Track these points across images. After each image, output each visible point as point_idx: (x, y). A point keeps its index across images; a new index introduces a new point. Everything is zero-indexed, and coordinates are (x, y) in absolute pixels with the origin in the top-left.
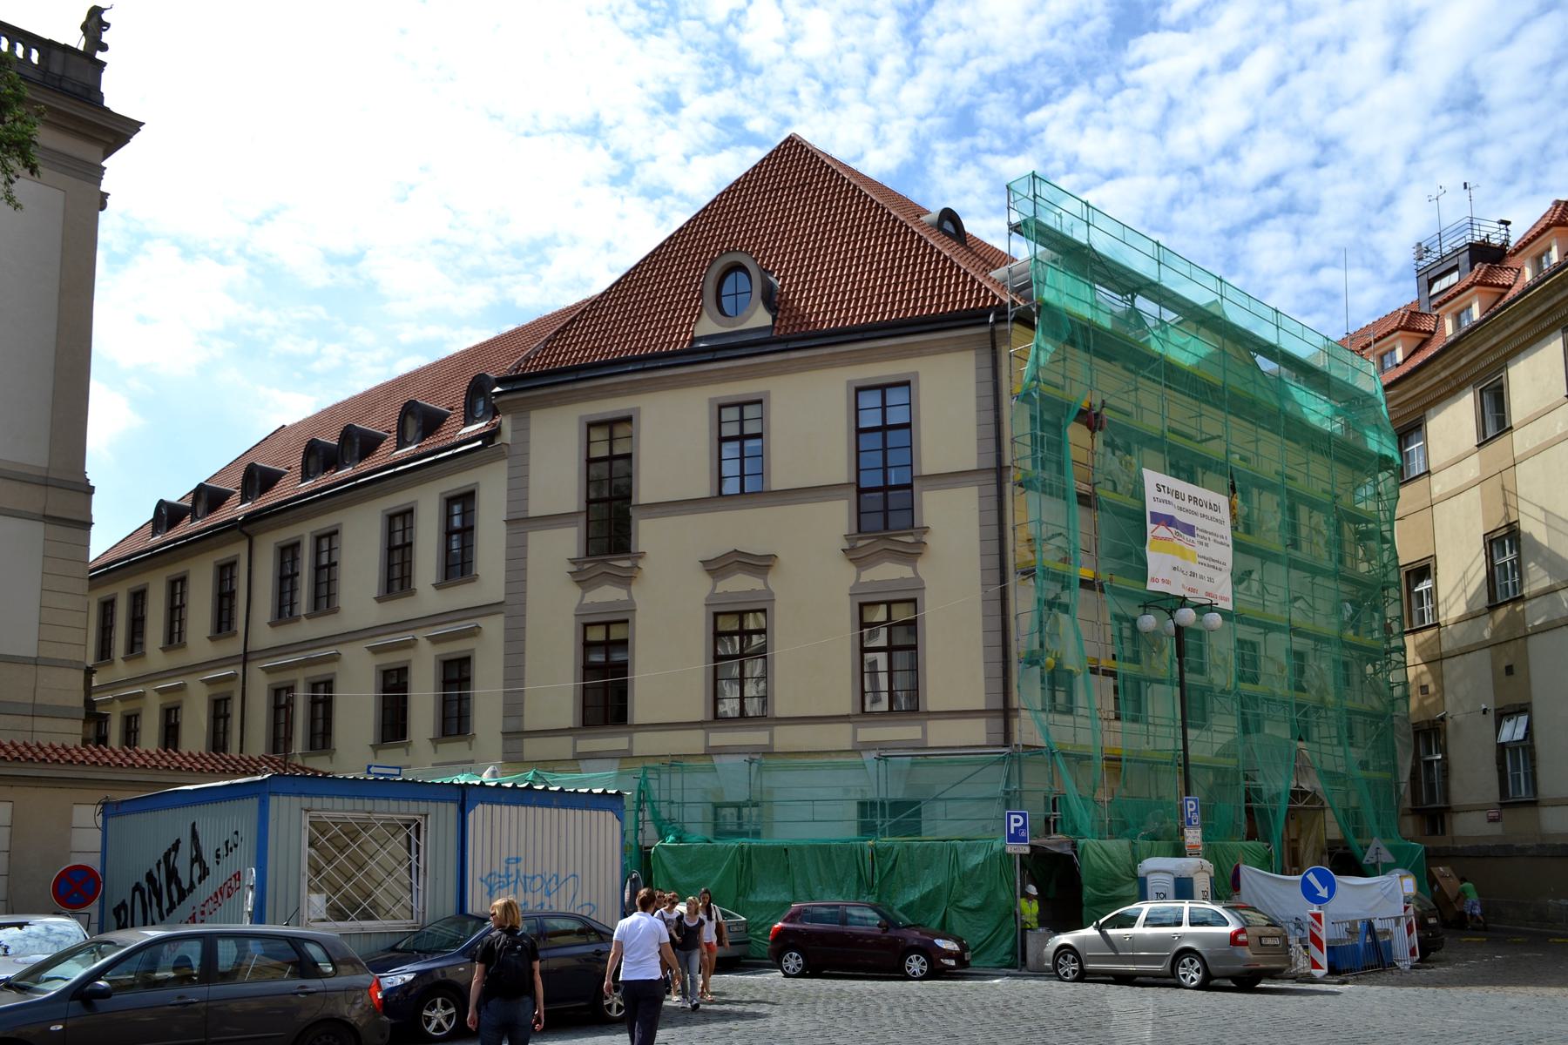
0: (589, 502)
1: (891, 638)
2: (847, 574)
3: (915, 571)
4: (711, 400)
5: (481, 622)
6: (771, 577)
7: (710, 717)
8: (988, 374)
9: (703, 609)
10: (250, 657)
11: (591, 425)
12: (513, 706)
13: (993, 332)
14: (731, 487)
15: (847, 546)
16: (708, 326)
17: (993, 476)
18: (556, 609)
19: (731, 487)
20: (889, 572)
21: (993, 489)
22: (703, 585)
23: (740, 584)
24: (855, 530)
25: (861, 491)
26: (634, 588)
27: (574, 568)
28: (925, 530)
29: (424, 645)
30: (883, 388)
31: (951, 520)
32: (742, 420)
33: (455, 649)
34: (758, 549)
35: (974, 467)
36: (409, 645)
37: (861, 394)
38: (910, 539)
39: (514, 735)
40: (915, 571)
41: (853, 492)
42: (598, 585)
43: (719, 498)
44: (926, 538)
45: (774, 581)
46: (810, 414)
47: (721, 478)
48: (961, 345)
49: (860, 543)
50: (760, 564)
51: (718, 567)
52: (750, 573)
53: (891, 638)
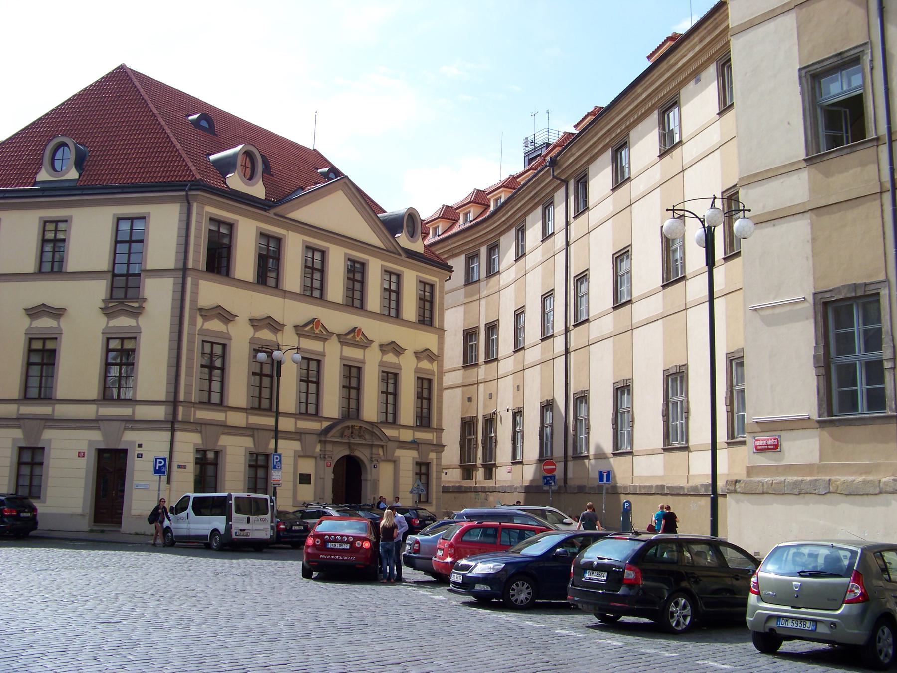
1: (121, 356)
2: (102, 322)
3: (137, 322)
4: (41, 218)
6: (62, 320)
8: (185, 219)
9: (24, 336)
13: (187, 195)
15: (102, 305)
16: (44, 176)
17: (181, 273)
19: (47, 267)
20: (123, 321)
21: (180, 280)
22: (26, 322)
23: (45, 323)
24: (108, 296)
25: (114, 275)
28: (144, 300)
31: (158, 294)
32: (56, 231)
34: (55, 303)
37: (120, 222)
38: (135, 305)
40: (137, 322)
41: (109, 276)
44: (144, 305)
45: (64, 323)
46: (91, 232)
47: (41, 262)
48: (173, 200)
49: (110, 305)
50: (57, 313)
51: (35, 312)
52: (50, 317)
53: (121, 356)
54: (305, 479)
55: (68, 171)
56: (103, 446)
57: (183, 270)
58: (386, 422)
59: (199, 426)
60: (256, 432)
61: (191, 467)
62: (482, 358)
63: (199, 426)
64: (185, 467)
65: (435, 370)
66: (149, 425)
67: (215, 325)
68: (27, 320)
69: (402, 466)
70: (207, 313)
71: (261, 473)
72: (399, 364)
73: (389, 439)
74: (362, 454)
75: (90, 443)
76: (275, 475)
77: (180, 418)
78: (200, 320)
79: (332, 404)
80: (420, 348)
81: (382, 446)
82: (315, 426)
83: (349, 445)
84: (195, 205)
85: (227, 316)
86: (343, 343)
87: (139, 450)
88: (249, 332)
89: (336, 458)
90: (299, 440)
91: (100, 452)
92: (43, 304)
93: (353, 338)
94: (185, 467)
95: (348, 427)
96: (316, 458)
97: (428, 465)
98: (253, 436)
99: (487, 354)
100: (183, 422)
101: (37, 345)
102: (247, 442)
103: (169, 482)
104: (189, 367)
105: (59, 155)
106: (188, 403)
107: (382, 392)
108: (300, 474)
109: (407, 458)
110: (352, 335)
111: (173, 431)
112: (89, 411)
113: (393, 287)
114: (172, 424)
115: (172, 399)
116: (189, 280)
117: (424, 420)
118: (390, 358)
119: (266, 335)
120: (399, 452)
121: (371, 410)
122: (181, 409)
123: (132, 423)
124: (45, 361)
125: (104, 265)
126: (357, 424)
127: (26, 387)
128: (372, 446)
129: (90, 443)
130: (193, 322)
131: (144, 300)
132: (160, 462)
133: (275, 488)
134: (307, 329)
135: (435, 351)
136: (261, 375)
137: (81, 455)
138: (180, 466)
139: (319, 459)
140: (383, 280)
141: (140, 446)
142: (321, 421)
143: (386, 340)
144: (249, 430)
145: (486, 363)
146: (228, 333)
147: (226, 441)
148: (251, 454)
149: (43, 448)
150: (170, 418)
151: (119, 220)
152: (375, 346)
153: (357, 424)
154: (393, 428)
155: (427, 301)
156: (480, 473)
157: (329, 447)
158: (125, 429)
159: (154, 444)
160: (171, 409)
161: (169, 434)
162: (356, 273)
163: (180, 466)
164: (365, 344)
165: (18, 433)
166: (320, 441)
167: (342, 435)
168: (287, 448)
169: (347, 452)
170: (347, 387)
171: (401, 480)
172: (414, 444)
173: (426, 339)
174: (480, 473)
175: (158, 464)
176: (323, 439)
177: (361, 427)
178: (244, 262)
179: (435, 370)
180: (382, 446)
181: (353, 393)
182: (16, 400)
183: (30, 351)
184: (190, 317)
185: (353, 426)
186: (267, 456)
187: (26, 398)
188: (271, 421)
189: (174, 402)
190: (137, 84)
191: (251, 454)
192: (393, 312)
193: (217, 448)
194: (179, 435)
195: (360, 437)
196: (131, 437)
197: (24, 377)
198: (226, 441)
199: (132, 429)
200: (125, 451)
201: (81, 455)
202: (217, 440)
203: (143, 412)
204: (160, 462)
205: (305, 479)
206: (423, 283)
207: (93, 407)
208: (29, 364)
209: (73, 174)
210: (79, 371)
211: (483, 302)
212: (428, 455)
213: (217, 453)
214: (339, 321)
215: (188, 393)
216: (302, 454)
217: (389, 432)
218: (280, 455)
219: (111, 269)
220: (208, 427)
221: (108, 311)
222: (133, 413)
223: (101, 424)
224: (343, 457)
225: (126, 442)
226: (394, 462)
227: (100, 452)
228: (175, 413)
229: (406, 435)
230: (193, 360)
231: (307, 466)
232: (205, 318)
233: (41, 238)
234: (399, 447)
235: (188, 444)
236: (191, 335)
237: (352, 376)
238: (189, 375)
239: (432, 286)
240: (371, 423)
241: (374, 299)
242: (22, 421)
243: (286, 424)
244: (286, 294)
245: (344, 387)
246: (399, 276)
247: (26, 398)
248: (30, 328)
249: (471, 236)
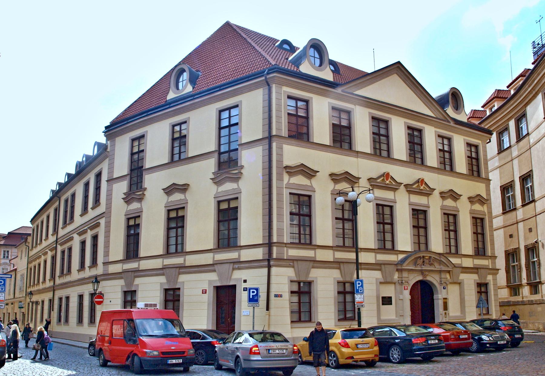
0: (132, 170)
2: (213, 189)
5: (100, 221)
7: (165, 252)
10: (58, 240)
11: (133, 140)
12: (107, 253)
14: (176, 157)
15: (213, 177)
16: (171, 96)
17: (267, 140)
18: (119, 211)
20: (229, 186)
23: (177, 197)
24: (217, 169)
25: (220, 154)
26: (143, 202)
27: (124, 196)
28: (242, 167)
29: (89, 230)
30: (229, 109)
31: (251, 160)
33: (94, 232)
35: (261, 137)
36: (85, 232)
37: (222, 113)
39: (104, 264)
41: (216, 155)
42: (132, 203)
43: (172, 162)
44: (242, 171)
50: (184, 188)
51: (170, 190)
54: (387, 301)
55: (186, 86)
56: (219, 284)
57: (269, 138)
58: (450, 253)
59: (292, 262)
60: (342, 265)
61: (286, 295)
62: (519, 203)
63: (292, 262)
64: (280, 296)
65: (486, 211)
66: (252, 264)
67: (300, 180)
68: (165, 197)
69: (466, 287)
70: (291, 171)
71: (349, 298)
72: (457, 207)
73: (454, 266)
74: (434, 279)
75: (210, 282)
76: (358, 298)
77: (274, 256)
78: (286, 177)
79: (404, 240)
80: (473, 194)
81: (449, 272)
82: (392, 258)
83: (422, 272)
84: (274, 88)
85: (308, 172)
86: (410, 192)
87: (244, 285)
88: (331, 186)
89: (412, 283)
90: (380, 270)
91: (218, 289)
92: (174, 184)
93: (419, 188)
94: (280, 296)
95: (420, 257)
96: (395, 283)
97: (486, 285)
98: (339, 268)
99: (523, 199)
100: (277, 259)
101: (173, 215)
102: (335, 274)
103: (268, 309)
104: (280, 215)
105: (181, 80)
106: (280, 244)
107: (445, 230)
108: (383, 298)
109: (470, 281)
110: (417, 185)
111: (269, 267)
112: (207, 259)
113: (446, 148)
114: (268, 262)
115: (267, 242)
116: (274, 145)
117: (480, 251)
118: (449, 202)
119: (343, 186)
120: (463, 276)
121: (437, 242)
122: (275, 249)
123: (237, 264)
124: (179, 225)
125: (212, 147)
126: (427, 255)
127: (168, 245)
128: (440, 272)
129: (210, 282)
130: (280, 178)
131: (242, 167)
132: (253, 292)
133: (359, 309)
134: (378, 181)
135: (485, 197)
136: (343, 219)
137: (204, 292)
138: (276, 296)
139: (397, 283)
140: (437, 143)
141: (245, 281)
142: (397, 254)
143: (446, 188)
144: (337, 264)
145: (523, 206)
146: (312, 186)
147: (316, 274)
148: (339, 282)
149: (179, 289)
150: (267, 257)
151: (221, 112)
152: (436, 193)
153: (427, 255)
154: (456, 257)
155: (474, 158)
156: (526, 291)
157: (405, 274)
158: (234, 269)
159: (255, 278)
160: (267, 249)
161: (265, 270)
162: (415, 139)
163: (276, 296)
164: (428, 192)
165: (162, 279)
166: (397, 270)
167: (415, 264)
168: (370, 278)
169: (420, 278)
170: (416, 227)
171: (466, 298)
172: (475, 270)
173: (476, 188)
174: (526, 291)
175: (251, 294)
176: (399, 267)
177: (430, 257)
178: (321, 131)
179: (486, 211)
180: (449, 272)
181: (422, 231)
182: (161, 255)
183: (169, 219)
184: (277, 174)
185: (423, 257)
186: (353, 284)
187: (168, 253)
188: (353, 256)
189: (269, 245)
190: (240, 32)
191: (339, 282)
192: (448, 168)
193: (309, 279)
194: (274, 270)
195: (431, 265)
196: (238, 276)
197: (166, 238)
198: (316, 274)
199: (239, 269)
200: (234, 287)
201: (204, 292)
202: (308, 273)
203: (246, 255)
204: (253, 292)
205: (387, 301)
206: (469, 145)
207: (211, 255)
208: (169, 229)
209: (189, 89)
210: (201, 230)
211: (516, 162)
212: (486, 277)
213: (310, 283)
214: (405, 174)
215: (280, 235)
216: (382, 281)
217: (455, 261)
218: (362, 281)
219: (217, 149)
220: (299, 262)
221: (217, 181)
222: (239, 256)
223: (216, 267)
224: (417, 282)
225: (236, 279)
226: (460, 283)
227: (218, 289)
228: (270, 253)
229: (468, 263)
230: (284, 207)
231: (389, 291)
232: (291, 174)
233: (171, 137)
234: (462, 272)
235: (283, 279)
236: (279, 188)
237: (419, 216)
238: (280, 219)
239: (476, 147)
240: (439, 254)
241: (432, 157)
242: (164, 270)
243: (364, 258)
244: (358, 154)
245: (414, 227)
246: (449, 139)
247: (168, 253)
248: (168, 202)
249: (500, 115)
